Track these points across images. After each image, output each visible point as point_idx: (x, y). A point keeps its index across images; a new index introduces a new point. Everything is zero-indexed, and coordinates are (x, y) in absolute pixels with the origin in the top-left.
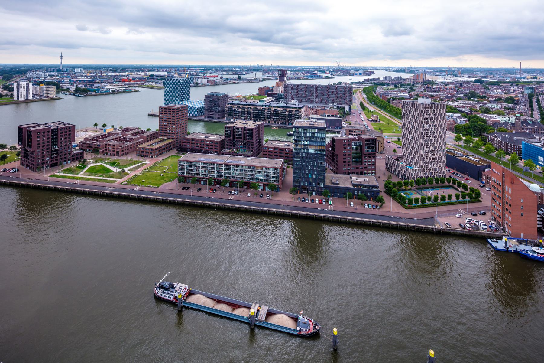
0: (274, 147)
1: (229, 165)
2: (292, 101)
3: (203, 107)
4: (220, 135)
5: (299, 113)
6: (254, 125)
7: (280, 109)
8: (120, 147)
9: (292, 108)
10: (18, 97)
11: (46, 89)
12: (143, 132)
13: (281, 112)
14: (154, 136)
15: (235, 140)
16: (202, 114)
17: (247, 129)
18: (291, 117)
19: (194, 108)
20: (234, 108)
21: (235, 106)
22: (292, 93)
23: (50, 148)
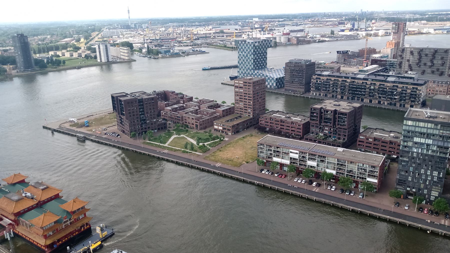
0: (374, 138)
1: (314, 155)
2: (409, 72)
3: (283, 77)
4: (304, 116)
5: (418, 92)
6: (348, 108)
7: (388, 85)
8: (198, 120)
9: (407, 83)
10: (101, 59)
11: (121, 50)
12: (218, 106)
13: (389, 89)
14: (230, 111)
15: (323, 124)
16: (281, 86)
17: (339, 113)
18: (405, 97)
19: (273, 79)
20: (323, 80)
21: (325, 78)
22: (411, 61)
23: (139, 118)
